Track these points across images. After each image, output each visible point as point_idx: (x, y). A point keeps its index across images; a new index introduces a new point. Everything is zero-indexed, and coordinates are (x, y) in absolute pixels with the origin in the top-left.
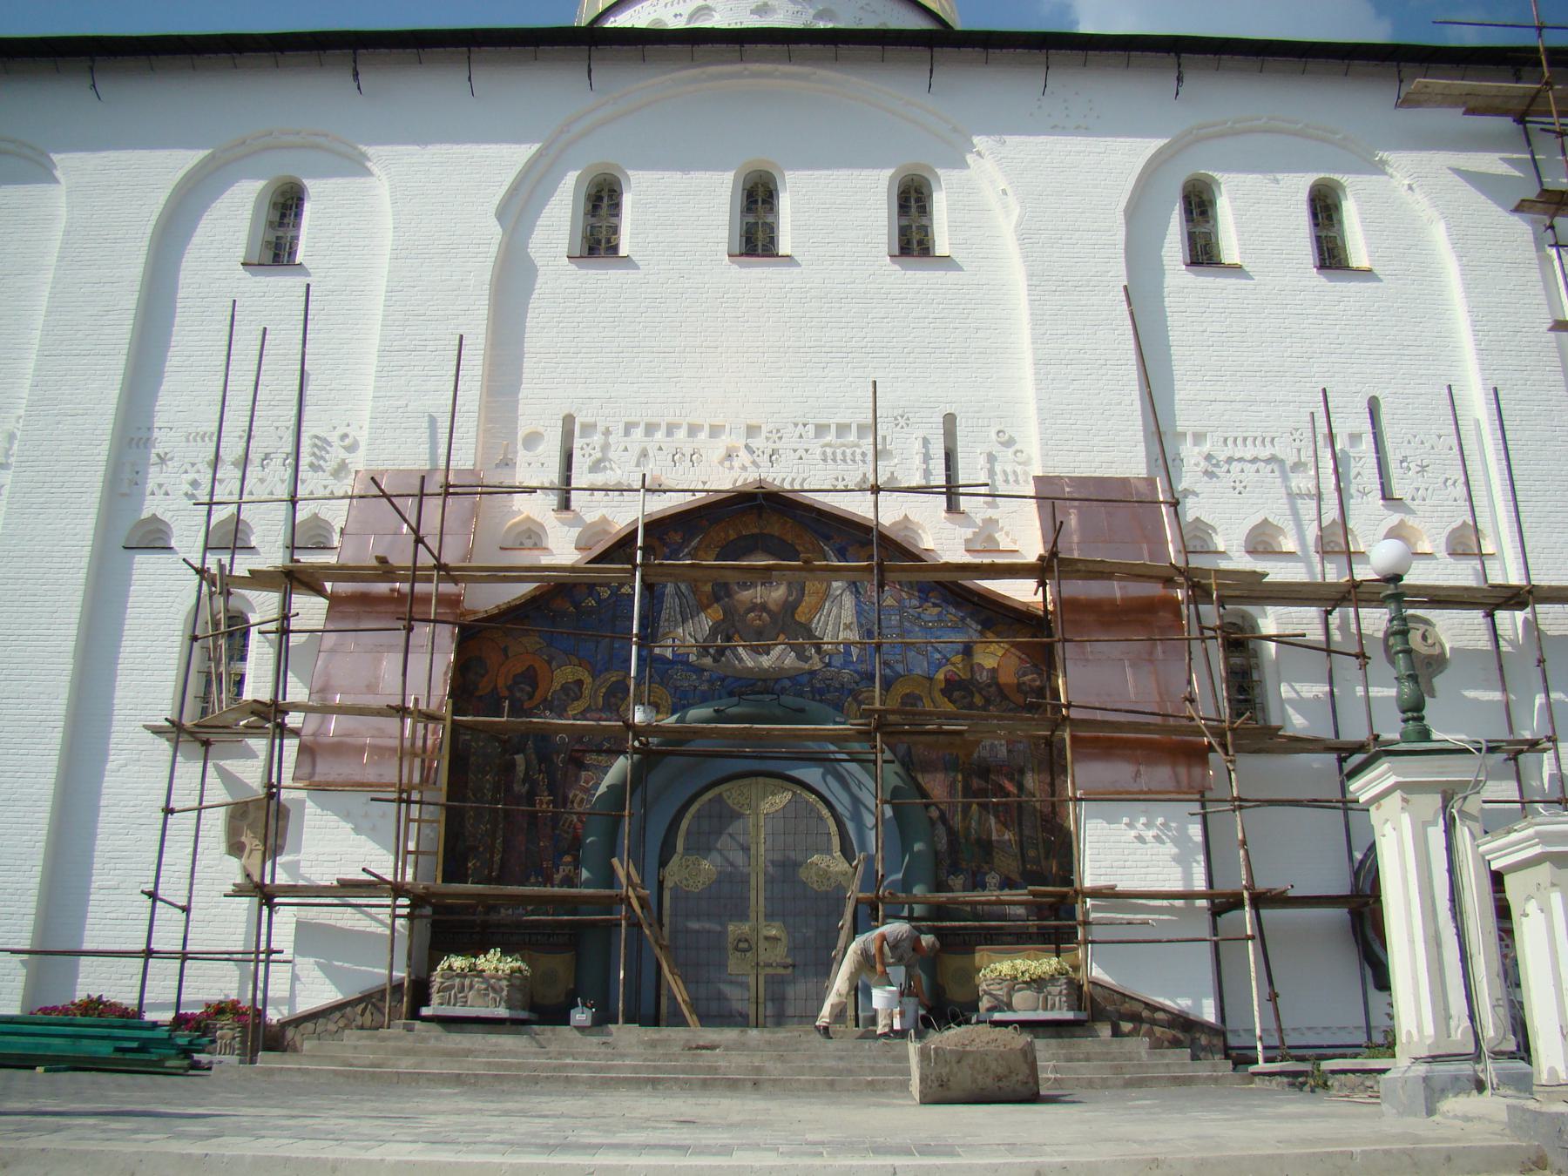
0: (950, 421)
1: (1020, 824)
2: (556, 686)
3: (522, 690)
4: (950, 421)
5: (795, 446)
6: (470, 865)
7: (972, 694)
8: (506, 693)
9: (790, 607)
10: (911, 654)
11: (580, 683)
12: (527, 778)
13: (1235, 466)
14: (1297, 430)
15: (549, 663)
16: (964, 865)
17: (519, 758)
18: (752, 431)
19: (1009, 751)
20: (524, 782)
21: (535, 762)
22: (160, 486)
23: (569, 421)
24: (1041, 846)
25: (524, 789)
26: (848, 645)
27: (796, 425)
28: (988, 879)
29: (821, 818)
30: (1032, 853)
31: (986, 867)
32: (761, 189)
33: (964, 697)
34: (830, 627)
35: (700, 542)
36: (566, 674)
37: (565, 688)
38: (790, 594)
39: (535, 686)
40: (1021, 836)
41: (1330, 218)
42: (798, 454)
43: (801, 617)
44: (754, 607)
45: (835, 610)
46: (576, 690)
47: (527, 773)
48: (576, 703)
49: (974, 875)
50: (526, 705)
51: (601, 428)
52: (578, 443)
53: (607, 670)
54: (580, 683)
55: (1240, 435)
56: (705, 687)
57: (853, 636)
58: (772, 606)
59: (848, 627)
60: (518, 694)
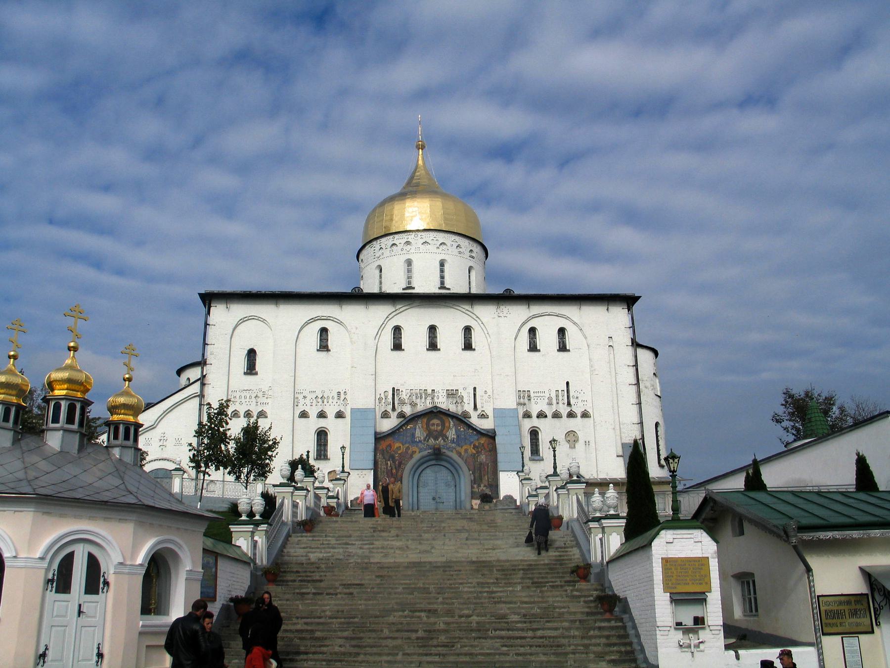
0: (475, 389)
2: (395, 447)
4: (475, 389)
9: (442, 430)
13: (536, 398)
17: (389, 462)
23: (393, 389)
25: (390, 468)
28: (482, 485)
30: (490, 480)
36: (397, 445)
44: (434, 431)
50: (390, 451)
51: (401, 391)
57: (455, 437)
58: (438, 431)
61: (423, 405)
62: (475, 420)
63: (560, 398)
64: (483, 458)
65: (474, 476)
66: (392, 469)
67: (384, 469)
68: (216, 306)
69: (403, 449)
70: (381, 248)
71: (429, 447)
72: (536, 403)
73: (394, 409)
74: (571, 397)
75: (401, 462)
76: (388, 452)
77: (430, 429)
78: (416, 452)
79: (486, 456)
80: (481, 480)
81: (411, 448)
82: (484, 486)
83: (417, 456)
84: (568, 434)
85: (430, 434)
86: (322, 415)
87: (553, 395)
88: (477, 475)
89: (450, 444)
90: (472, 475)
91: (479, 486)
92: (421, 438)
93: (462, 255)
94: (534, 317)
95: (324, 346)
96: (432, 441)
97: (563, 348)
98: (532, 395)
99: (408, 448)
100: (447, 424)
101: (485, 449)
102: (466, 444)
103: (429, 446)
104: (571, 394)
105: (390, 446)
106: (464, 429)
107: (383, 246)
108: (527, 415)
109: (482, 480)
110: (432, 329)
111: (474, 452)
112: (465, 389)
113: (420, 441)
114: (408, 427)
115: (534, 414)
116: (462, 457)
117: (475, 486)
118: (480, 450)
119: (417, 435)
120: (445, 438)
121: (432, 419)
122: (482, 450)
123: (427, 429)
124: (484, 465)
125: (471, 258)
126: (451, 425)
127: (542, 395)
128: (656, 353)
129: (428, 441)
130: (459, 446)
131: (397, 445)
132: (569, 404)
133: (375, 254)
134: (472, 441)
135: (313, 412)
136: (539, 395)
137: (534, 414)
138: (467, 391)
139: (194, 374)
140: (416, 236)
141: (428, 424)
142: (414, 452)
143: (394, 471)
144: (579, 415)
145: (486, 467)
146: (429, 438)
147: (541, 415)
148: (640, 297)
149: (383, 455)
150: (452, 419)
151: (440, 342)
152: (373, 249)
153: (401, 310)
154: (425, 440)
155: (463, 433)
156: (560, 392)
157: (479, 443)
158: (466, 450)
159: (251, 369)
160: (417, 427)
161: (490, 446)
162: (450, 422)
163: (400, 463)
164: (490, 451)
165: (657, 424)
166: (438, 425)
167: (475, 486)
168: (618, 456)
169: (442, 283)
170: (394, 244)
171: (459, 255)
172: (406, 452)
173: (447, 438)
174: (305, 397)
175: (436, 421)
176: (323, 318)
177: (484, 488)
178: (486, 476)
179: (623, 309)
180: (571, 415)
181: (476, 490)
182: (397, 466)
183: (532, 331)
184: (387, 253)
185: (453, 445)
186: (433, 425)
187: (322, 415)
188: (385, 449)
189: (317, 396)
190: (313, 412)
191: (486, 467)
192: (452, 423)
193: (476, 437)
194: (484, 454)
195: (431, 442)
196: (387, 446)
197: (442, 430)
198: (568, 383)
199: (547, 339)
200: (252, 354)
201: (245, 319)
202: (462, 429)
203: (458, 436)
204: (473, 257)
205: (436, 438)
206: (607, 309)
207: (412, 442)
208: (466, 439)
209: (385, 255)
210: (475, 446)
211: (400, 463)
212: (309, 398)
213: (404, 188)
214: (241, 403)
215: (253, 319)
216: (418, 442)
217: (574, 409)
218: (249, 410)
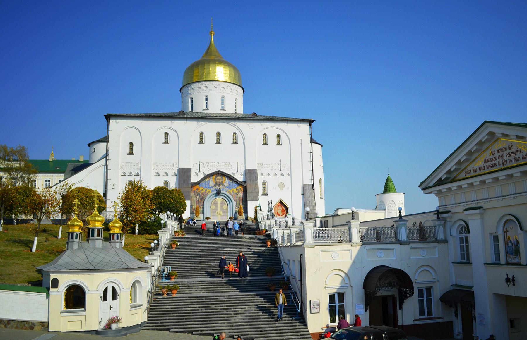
0: (237, 162)
2: (200, 190)
4: (237, 162)
9: (222, 182)
12: (198, 198)
13: (265, 167)
17: (197, 197)
29: (224, 202)
36: (201, 189)
44: (218, 182)
52: (201, 164)
56: (214, 190)
57: (228, 185)
66: (198, 200)
69: (204, 191)
73: (199, 171)
76: (197, 192)
85: (216, 184)
87: (273, 166)
88: (238, 202)
89: (226, 188)
90: (236, 203)
93: (232, 93)
94: (266, 128)
95: (166, 142)
99: (206, 190)
102: (233, 188)
105: (198, 189)
107: (193, 87)
110: (218, 134)
112: (233, 162)
113: (212, 187)
114: (206, 180)
115: (265, 174)
117: (237, 208)
118: (239, 191)
119: (210, 184)
120: (223, 185)
121: (218, 176)
127: (268, 166)
128: (321, 145)
129: (215, 187)
137: (265, 174)
139: (101, 148)
141: (215, 179)
142: (209, 192)
143: (200, 201)
146: (216, 185)
147: (269, 175)
148: (315, 121)
149: (194, 193)
150: (227, 176)
151: (223, 140)
153: (203, 124)
154: (214, 186)
155: (232, 183)
158: (233, 191)
159: (131, 153)
160: (211, 180)
163: (202, 197)
165: (320, 179)
166: (220, 179)
167: (237, 208)
168: (302, 194)
169: (223, 107)
174: (157, 166)
175: (219, 177)
176: (166, 127)
180: (282, 175)
182: (201, 198)
183: (265, 135)
185: (227, 189)
186: (218, 179)
190: (162, 173)
192: (226, 179)
197: (222, 182)
199: (272, 140)
200: (131, 144)
201: (127, 128)
203: (229, 185)
204: (237, 94)
205: (219, 186)
207: (208, 187)
208: (233, 186)
210: (237, 189)
211: (202, 197)
213: (203, 57)
214: (126, 169)
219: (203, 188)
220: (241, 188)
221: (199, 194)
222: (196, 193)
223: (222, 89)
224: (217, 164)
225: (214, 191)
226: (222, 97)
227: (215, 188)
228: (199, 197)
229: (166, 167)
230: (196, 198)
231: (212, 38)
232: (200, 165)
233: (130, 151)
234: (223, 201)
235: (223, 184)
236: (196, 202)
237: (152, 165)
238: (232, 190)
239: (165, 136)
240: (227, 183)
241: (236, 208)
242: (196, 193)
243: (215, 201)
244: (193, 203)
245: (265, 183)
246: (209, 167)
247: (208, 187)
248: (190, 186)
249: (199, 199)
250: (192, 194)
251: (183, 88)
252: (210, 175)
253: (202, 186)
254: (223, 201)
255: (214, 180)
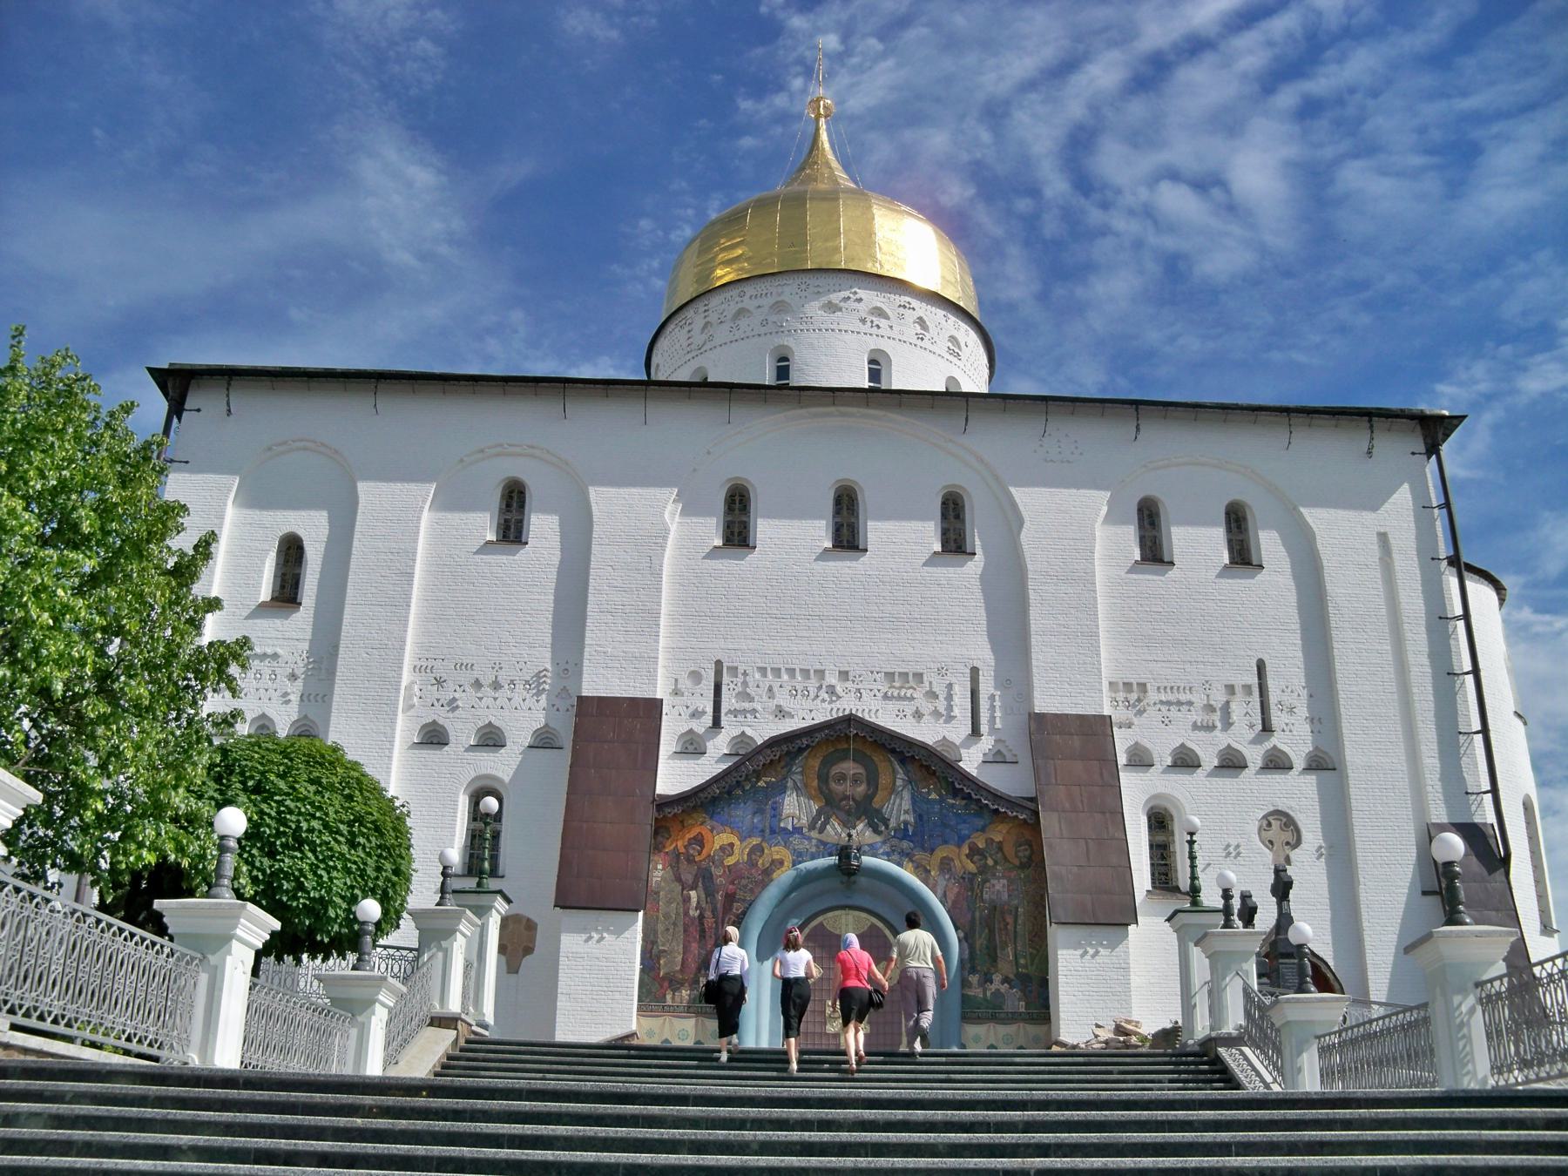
1: (1015, 944)
2: (717, 846)
3: (694, 849)
5: (871, 687)
6: (661, 962)
7: (986, 858)
8: (682, 850)
9: (869, 798)
10: (948, 831)
11: (732, 845)
13: (1163, 708)
14: (1207, 682)
15: (712, 831)
16: (979, 968)
17: (693, 894)
18: (844, 675)
19: (1009, 896)
20: (696, 909)
21: (704, 896)
22: (438, 700)
23: (719, 664)
24: (1028, 957)
25: (697, 913)
26: (906, 823)
27: (872, 672)
28: (994, 977)
30: (1022, 961)
31: (993, 970)
32: (846, 498)
33: (981, 860)
34: (895, 812)
35: (809, 753)
37: (722, 848)
38: (869, 789)
39: (702, 847)
40: (1016, 948)
41: (1239, 527)
42: (873, 693)
43: (876, 804)
44: (846, 798)
45: (898, 801)
46: (729, 849)
47: (698, 902)
48: (729, 858)
49: (986, 974)
50: (697, 859)
51: (741, 670)
52: (726, 679)
53: (750, 837)
54: (732, 845)
55: (1169, 685)
56: (814, 850)
57: (911, 818)
59: (906, 812)
60: (691, 852)
61: (809, 713)
62: (971, 762)
63: (1237, 710)
64: (998, 888)
65: (972, 948)
66: (701, 917)
67: (677, 914)
68: (199, 410)
70: (707, 324)
71: (824, 849)
72: (1167, 722)
73: (717, 723)
74: (1272, 706)
75: (735, 893)
76: (690, 860)
77: (829, 790)
78: (781, 863)
79: (1011, 882)
80: (994, 959)
81: (766, 851)
82: (1006, 980)
83: (785, 876)
84: (1266, 823)
86: (491, 739)
88: (980, 942)
91: (988, 979)
92: (799, 819)
96: (835, 831)
97: (1242, 556)
98: (1153, 696)
100: (884, 780)
101: (1006, 859)
102: (945, 842)
103: (824, 844)
104: (1273, 697)
105: (699, 841)
106: (940, 795)
107: (713, 317)
108: (1141, 760)
109: (995, 961)
111: (972, 867)
113: (797, 830)
114: (761, 784)
115: (1163, 753)
116: (931, 881)
117: (974, 979)
118: (990, 862)
121: (845, 758)
122: (996, 863)
123: (821, 792)
124: (1003, 913)
125: (951, 358)
126: (899, 782)
127: (1183, 697)
129: (822, 830)
130: (924, 849)
131: (723, 838)
132: (1267, 728)
133: (689, 342)
134: (967, 832)
135: (462, 733)
136: (1172, 697)
138: (950, 678)
140: (803, 287)
141: (823, 778)
143: (709, 921)
144: (1299, 763)
145: (1010, 919)
147: (1185, 761)
150: (903, 760)
152: (687, 328)
154: (812, 827)
155: (937, 807)
156: (1238, 689)
157: (990, 841)
159: (287, 593)
160: (790, 784)
161: (1024, 852)
162: (894, 772)
163: (730, 898)
164: (1023, 866)
168: (1425, 893)
170: (741, 313)
171: (919, 343)
172: (752, 863)
173: (886, 822)
174: (439, 682)
175: (850, 767)
176: (511, 449)
177: (1004, 988)
178: (1010, 950)
179: (1413, 453)
180: (1276, 763)
181: (976, 992)
182: (719, 906)
184: (721, 334)
185: (905, 844)
186: (842, 778)
187: (491, 739)
188: (682, 850)
189: (477, 681)
190: (462, 733)
191: (1010, 919)
193: (979, 822)
194: (1003, 877)
195: (833, 833)
196: (690, 844)
197: (869, 798)
198: (1261, 666)
202: (933, 796)
203: (920, 817)
206: (1369, 453)
207: (773, 832)
208: (945, 825)
209: (717, 341)
212: (450, 685)
215: (305, 449)
216: (791, 833)
217: (1276, 740)
218: (263, 716)
219: (735, 830)
220: (1000, 846)
221: (704, 878)
222: (684, 865)
223: (869, 318)
224: (831, 679)
225: (813, 857)
226: (871, 362)
227: (823, 837)
228: (710, 893)
229: (489, 692)
230: (687, 900)
231: (824, 136)
232: (724, 689)
233: (283, 587)
234: (873, 926)
235: (878, 812)
236: (685, 931)
237: (406, 676)
238: (941, 852)
239: (508, 505)
240: (906, 805)
241: (965, 983)
242: (684, 865)
243: (821, 924)
244: (660, 939)
245: (1159, 821)
246: (783, 699)
247: (773, 832)
248: (648, 817)
249: (708, 914)
250: (659, 872)
251: (663, 344)
252: (788, 748)
253: (728, 824)
254: (873, 926)
255: (815, 783)
